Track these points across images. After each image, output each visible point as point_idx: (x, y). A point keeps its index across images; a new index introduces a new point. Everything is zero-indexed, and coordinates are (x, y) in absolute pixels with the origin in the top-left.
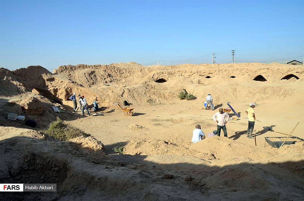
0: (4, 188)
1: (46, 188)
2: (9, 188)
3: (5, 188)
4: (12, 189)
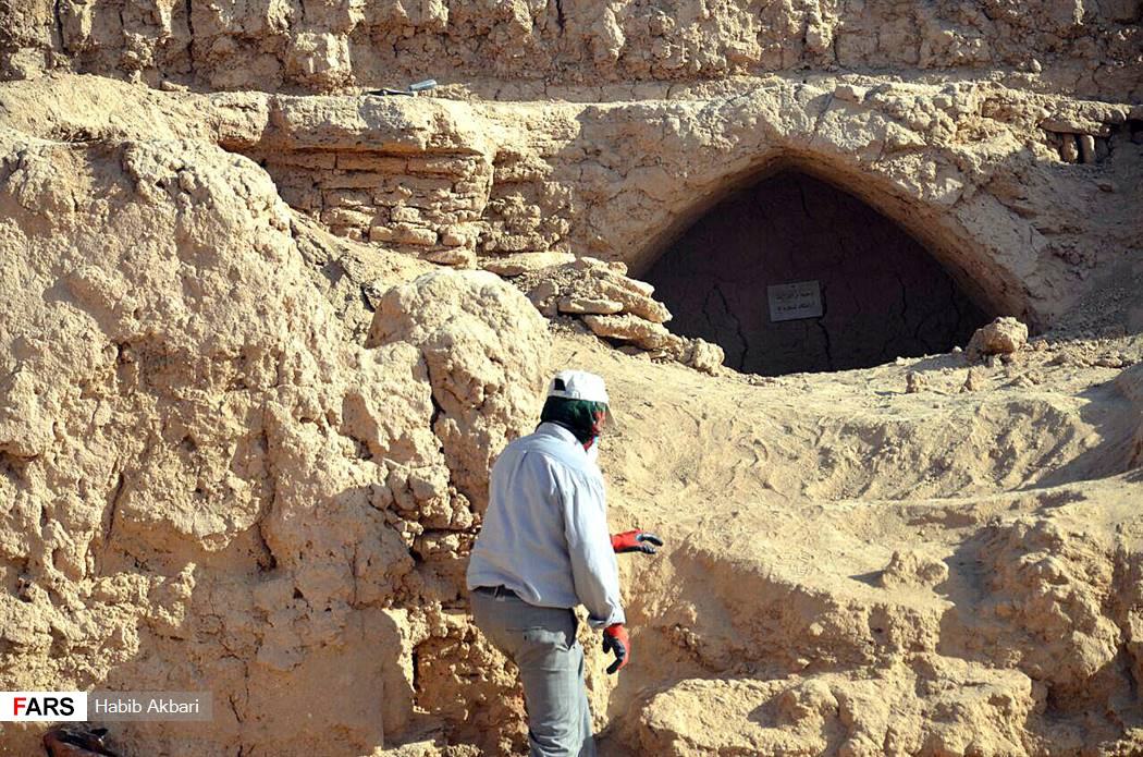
0: (16, 706)
1: (174, 708)
2: (34, 707)
3: (19, 710)
4: (46, 713)
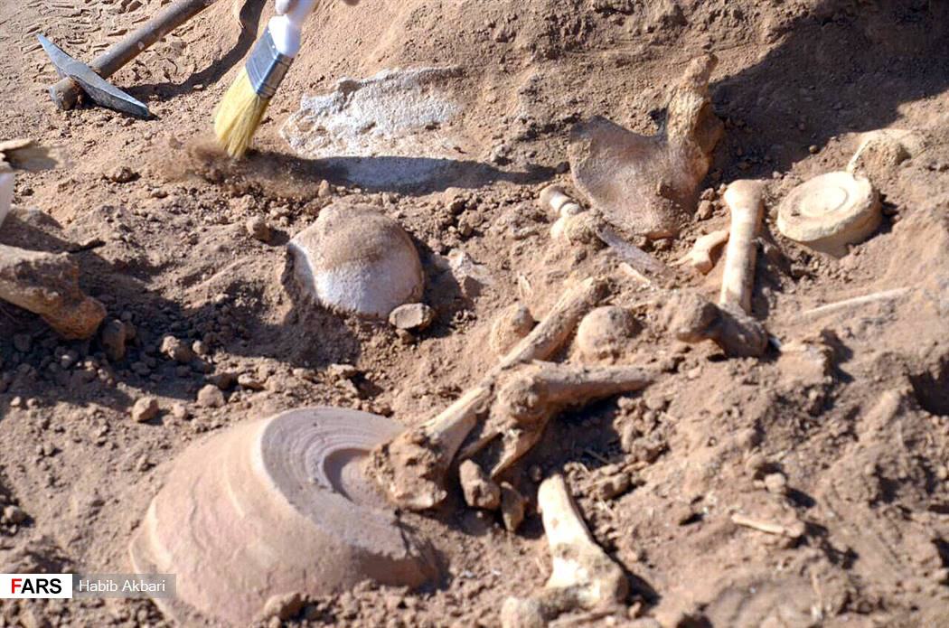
0: (14, 586)
2: (28, 586)
3: (16, 589)
4: (38, 592)
